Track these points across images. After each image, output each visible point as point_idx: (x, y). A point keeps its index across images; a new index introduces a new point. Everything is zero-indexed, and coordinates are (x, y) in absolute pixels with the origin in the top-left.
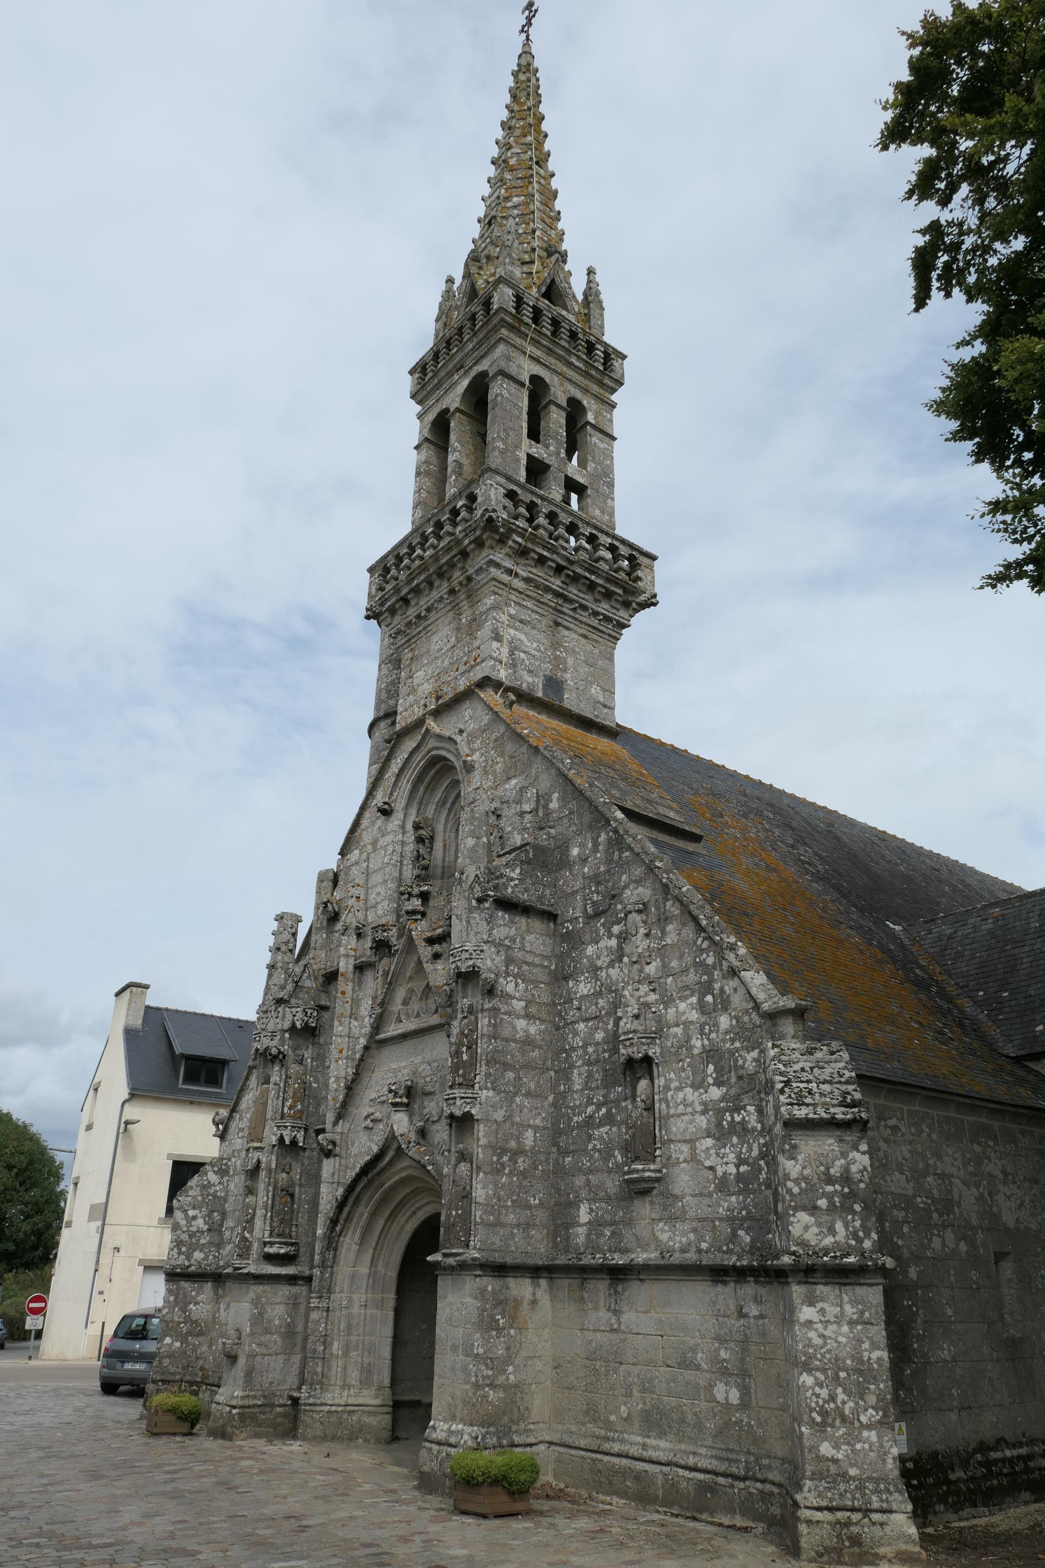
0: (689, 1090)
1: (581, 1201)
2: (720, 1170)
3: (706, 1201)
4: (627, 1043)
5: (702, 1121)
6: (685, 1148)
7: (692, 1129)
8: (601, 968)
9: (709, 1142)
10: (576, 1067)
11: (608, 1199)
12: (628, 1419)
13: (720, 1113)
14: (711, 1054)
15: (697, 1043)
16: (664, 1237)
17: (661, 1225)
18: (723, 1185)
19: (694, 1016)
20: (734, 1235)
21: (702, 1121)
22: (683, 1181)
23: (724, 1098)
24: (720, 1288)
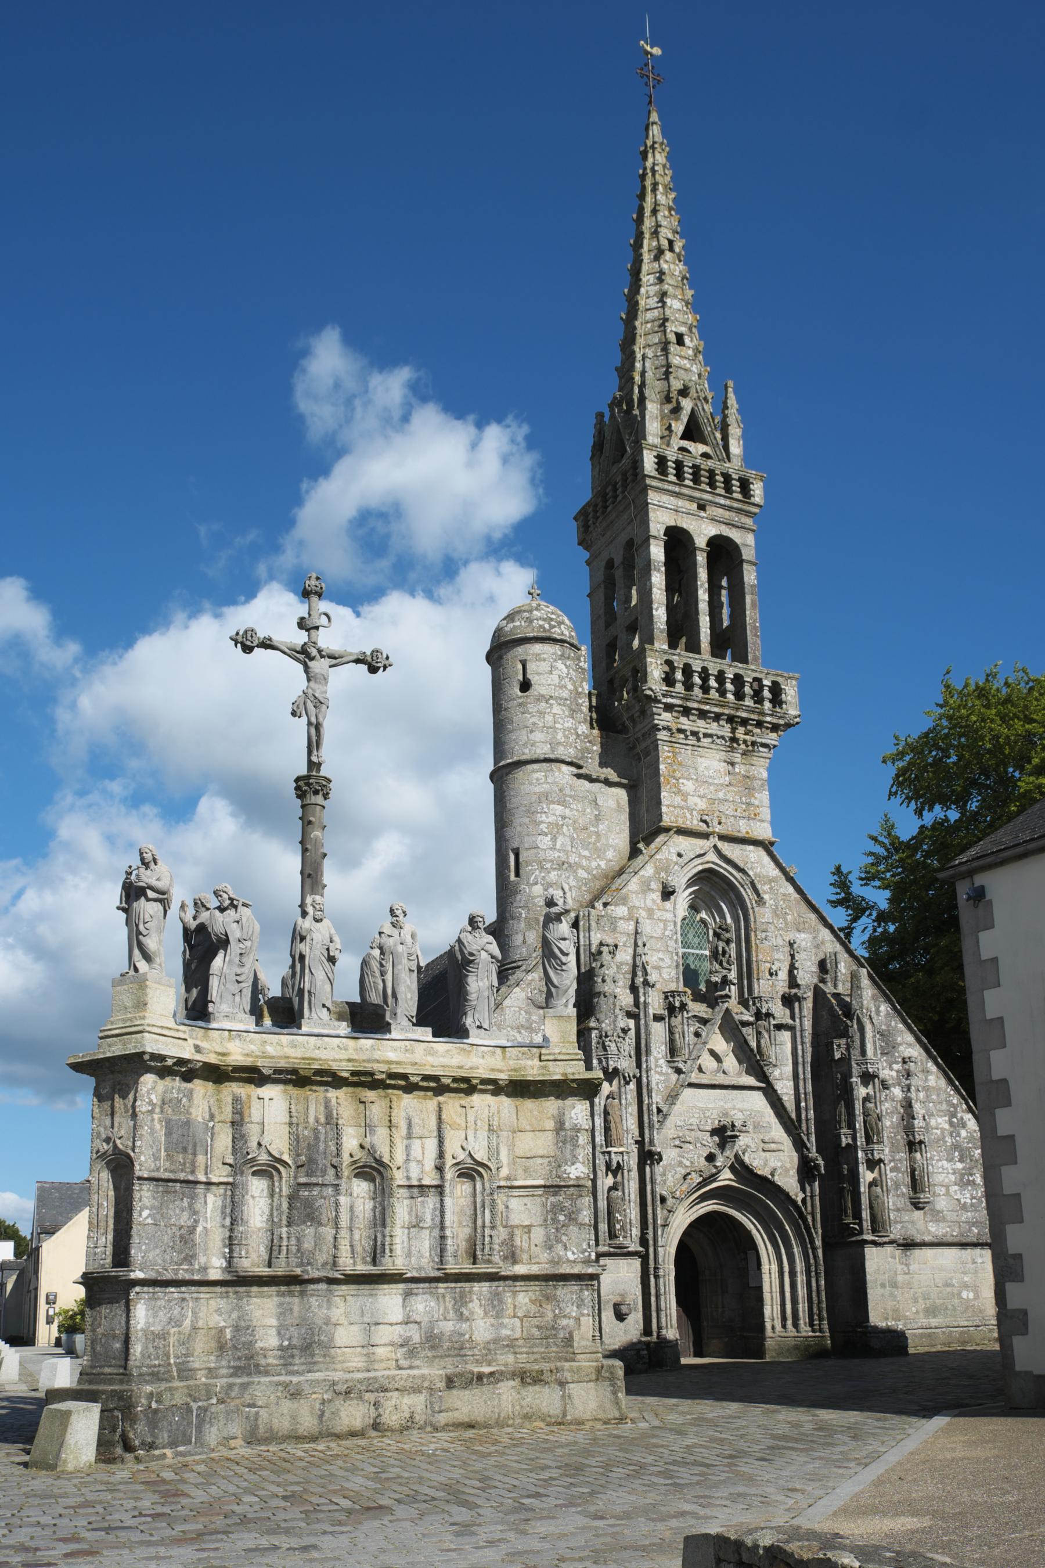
0: (945, 1162)
2: (962, 1201)
3: (955, 1214)
5: (953, 1178)
6: (943, 1189)
7: (947, 1180)
9: (956, 1188)
11: (898, 1210)
12: (917, 1312)
13: (962, 1175)
14: (956, 1147)
15: (949, 1140)
16: (933, 1229)
18: (964, 1207)
19: (947, 1126)
20: (970, 1230)
21: (953, 1178)
22: (942, 1203)
23: (963, 1169)
24: (963, 1251)
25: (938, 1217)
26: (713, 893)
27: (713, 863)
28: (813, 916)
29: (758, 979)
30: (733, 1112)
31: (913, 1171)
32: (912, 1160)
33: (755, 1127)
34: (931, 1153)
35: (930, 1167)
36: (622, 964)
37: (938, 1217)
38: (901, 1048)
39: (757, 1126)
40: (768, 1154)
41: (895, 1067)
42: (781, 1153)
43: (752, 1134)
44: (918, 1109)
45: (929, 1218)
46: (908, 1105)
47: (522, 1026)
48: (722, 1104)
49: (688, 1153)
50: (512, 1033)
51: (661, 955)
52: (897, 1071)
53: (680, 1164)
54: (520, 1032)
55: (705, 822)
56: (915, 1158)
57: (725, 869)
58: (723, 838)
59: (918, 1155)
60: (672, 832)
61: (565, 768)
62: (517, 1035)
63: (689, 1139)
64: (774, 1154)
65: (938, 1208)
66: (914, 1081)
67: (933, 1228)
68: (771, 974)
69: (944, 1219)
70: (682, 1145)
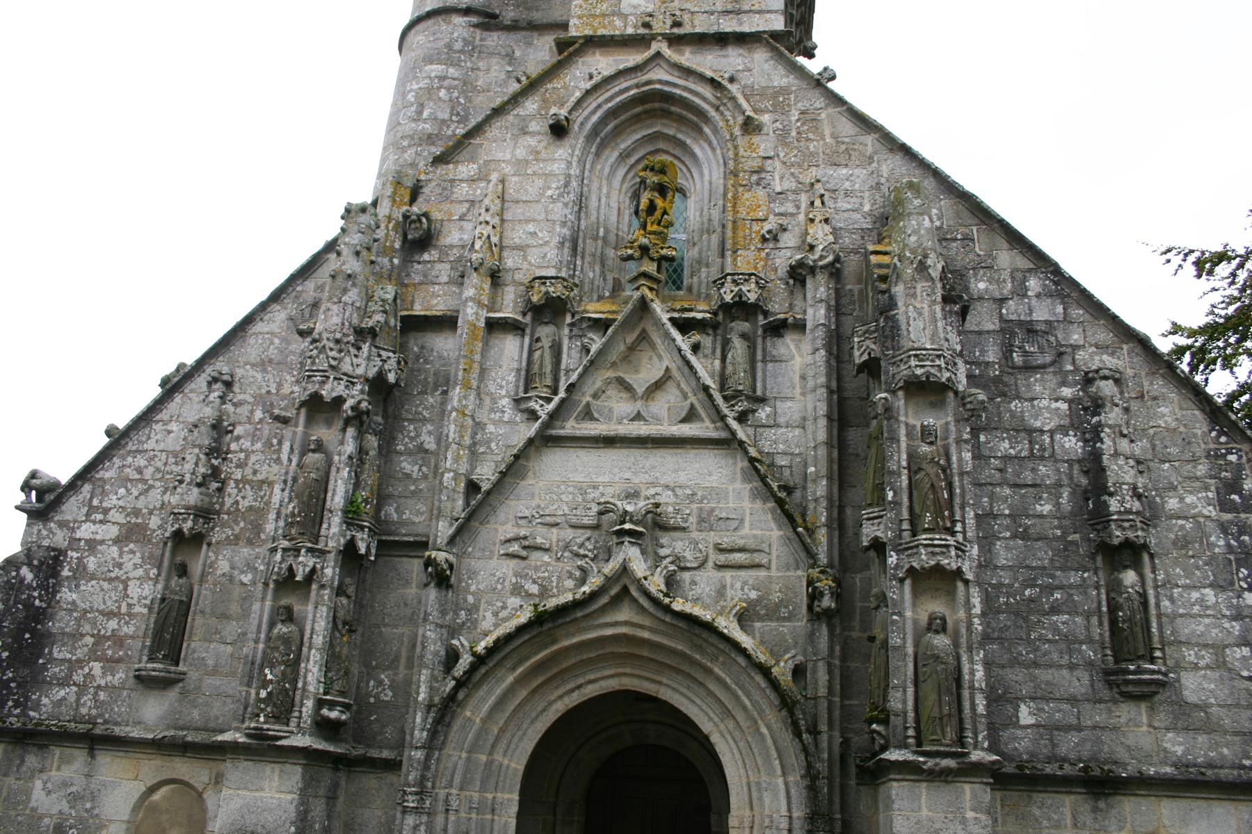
1: (1022, 699)
4: (1126, 525)
8: (1042, 432)
10: (999, 539)
17: (1170, 735)
25: (1187, 717)
26: (680, 136)
27: (660, 82)
28: (870, 140)
29: (735, 252)
30: (652, 491)
31: (1113, 608)
32: (1114, 587)
33: (701, 520)
34: (1169, 568)
35: (1166, 603)
36: (451, 247)
37: (1187, 717)
38: (1081, 355)
39: (706, 521)
40: (728, 575)
41: (1067, 392)
42: (762, 573)
43: (695, 535)
44: (1120, 472)
45: (1162, 719)
46: (1093, 465)
47: (270, 361)
48: (627, 475)
49: (537, 569)
50: (251, 373)
51: (531, 227)
52: (1070, 401)
53: (517, 590)
54: (264, 371)
55: (647, 25)
56: (1119, 583)
57: (685, 89)
58: (676, 41)
59: (1130, 577)
60: (577, 46)
61: (458, 20)
62: (259, 376)
63: (539, 540)
64: (742, 573)
65: (1190, 695)
66: (1112, 416)
67: (1176, 745)
68: (764, 240)
69: (1209, 727)
70: (524, 553)
